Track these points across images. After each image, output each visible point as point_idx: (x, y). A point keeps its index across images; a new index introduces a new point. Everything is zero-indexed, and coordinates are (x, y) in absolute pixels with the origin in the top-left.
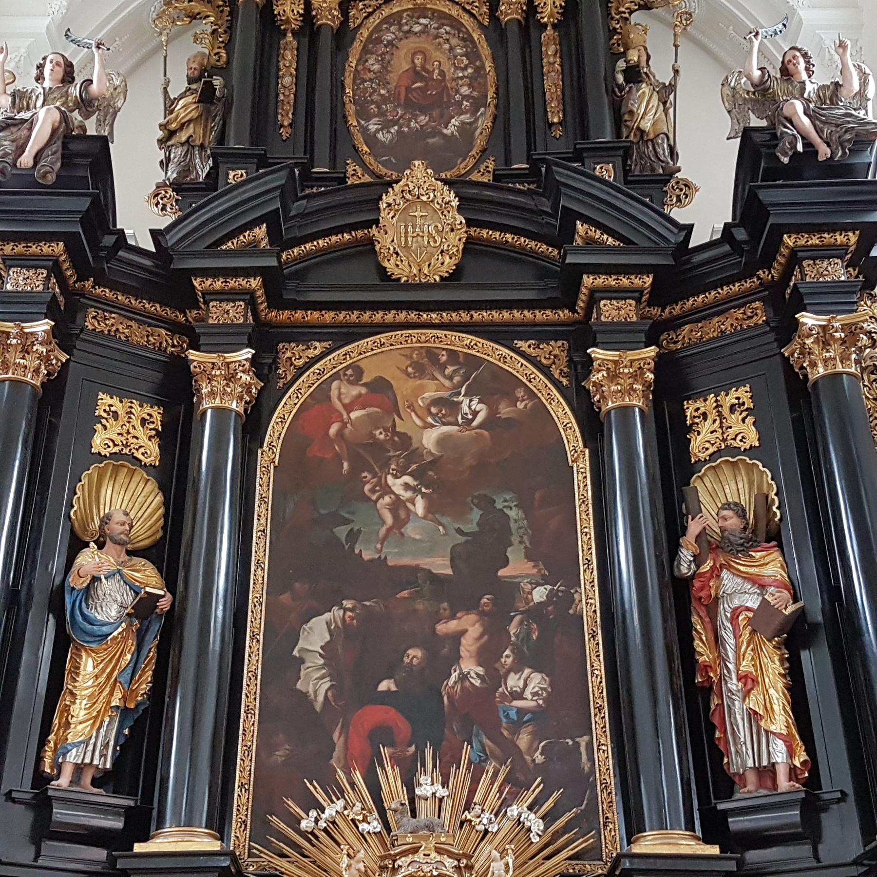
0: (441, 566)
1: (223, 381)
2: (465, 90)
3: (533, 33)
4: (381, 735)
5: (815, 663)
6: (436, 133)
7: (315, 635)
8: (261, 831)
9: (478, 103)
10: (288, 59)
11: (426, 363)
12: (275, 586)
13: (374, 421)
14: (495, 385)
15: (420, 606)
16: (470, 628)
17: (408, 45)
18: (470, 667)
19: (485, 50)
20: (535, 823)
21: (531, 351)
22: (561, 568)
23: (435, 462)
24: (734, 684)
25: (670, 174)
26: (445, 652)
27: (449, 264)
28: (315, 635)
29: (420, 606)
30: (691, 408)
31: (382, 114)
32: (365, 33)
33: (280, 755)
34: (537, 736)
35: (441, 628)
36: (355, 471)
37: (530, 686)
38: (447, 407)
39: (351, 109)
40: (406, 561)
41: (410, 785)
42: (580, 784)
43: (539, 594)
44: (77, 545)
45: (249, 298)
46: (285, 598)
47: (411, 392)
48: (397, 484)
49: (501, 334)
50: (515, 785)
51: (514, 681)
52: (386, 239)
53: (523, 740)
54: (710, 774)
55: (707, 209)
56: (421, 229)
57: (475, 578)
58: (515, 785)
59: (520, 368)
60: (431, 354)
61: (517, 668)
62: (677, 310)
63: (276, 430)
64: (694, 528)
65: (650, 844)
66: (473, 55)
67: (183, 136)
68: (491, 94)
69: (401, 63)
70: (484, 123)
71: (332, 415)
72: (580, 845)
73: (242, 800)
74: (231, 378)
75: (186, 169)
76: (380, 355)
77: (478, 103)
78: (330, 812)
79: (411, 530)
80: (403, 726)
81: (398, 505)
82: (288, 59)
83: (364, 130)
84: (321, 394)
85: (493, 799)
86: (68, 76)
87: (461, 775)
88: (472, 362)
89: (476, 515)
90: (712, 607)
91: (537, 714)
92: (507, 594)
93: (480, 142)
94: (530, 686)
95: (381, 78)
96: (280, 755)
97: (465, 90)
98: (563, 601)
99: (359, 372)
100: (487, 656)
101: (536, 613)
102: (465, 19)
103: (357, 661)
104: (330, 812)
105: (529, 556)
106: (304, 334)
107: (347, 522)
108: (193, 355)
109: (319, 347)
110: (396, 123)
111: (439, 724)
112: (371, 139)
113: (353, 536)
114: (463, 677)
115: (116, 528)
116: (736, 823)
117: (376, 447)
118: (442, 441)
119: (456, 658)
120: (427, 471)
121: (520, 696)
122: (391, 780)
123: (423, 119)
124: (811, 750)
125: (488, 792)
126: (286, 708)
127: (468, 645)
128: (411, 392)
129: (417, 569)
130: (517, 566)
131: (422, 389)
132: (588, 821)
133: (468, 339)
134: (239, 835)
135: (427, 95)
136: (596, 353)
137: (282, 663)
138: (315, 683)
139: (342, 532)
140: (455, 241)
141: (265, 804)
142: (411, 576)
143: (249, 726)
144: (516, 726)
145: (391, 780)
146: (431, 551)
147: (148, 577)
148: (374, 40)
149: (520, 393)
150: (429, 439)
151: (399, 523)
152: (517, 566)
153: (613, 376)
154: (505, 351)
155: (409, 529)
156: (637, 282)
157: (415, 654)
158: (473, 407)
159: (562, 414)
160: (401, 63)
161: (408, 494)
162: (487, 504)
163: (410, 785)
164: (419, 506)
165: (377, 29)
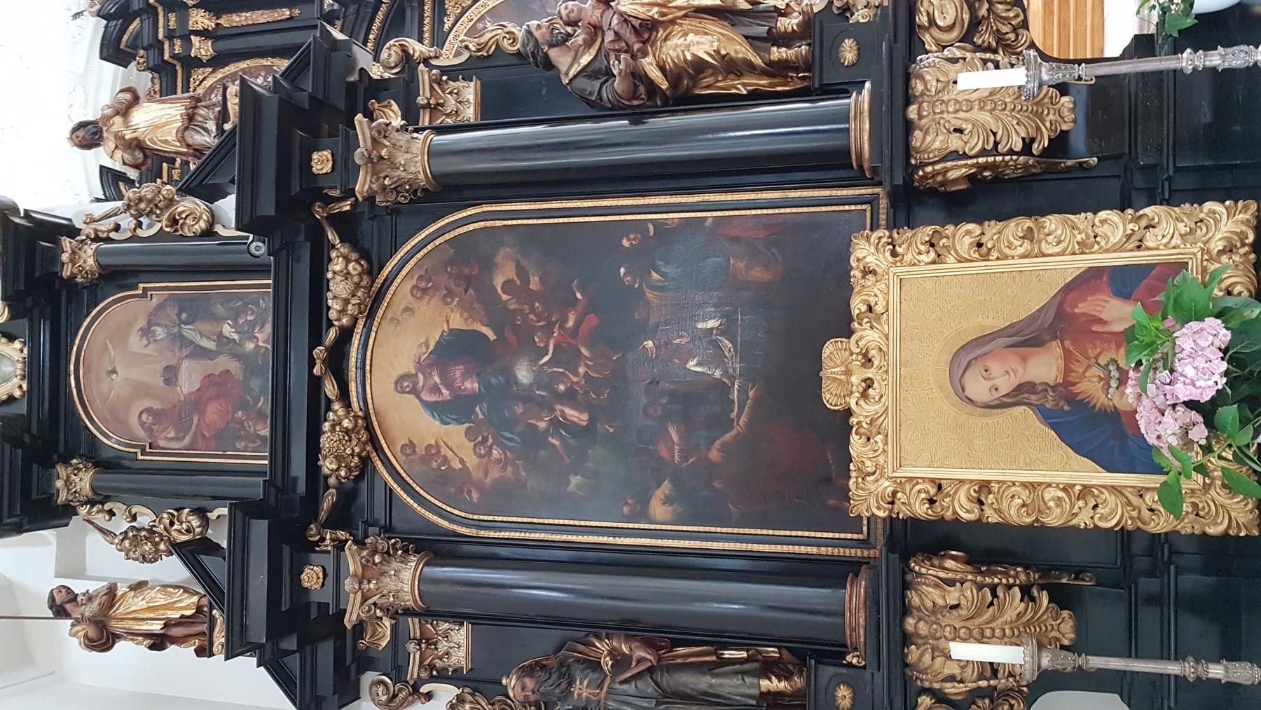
3: (220, 33)
21: (452, 19)
59: (465, 24)
68: (265, 62)
102: (207, 84)
149: (480, 26)
154: (451, 36)
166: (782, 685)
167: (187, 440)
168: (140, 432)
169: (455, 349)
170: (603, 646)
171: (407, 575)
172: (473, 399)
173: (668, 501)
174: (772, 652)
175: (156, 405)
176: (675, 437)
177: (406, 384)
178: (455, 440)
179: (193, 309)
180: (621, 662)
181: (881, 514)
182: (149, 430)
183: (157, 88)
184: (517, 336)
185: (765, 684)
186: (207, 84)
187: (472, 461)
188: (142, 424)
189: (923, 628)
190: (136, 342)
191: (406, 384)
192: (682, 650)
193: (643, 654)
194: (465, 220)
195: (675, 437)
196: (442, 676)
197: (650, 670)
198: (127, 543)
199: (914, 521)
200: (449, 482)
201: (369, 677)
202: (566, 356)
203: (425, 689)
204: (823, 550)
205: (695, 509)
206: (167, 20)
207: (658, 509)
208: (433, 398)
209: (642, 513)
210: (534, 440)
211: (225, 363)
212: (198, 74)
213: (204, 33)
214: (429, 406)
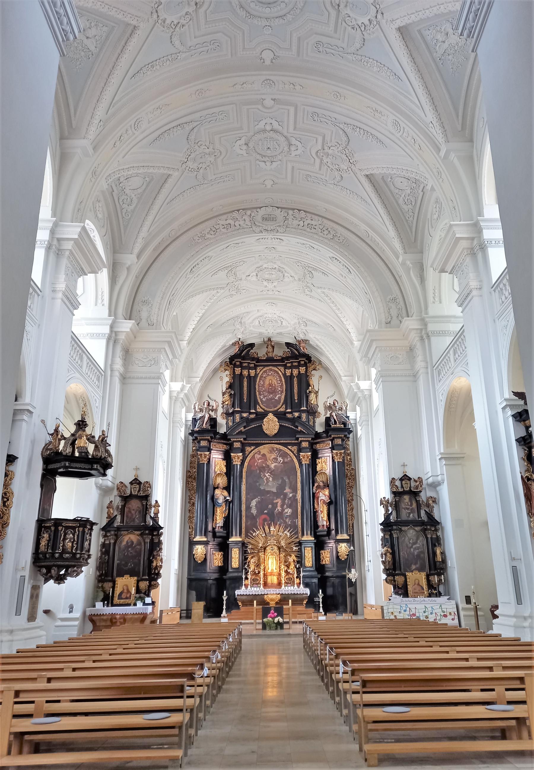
0: (274, 490)
1: (237, 458)
2: (279, 389)
4: (265, 520)
5: (332, 508)
6: (274, 399)
7: (254, 503)
8: (247, 536)
9: (282, 392)
10: (245, 384)
11: (272, 451)
12: (247, 494)
13: (263, 462)
14: (284, 455)
15: (271, 498)
16: (279, 501)
17: (268, 378)
18: (279, 508)
19: (283, 380)
20: (288, 534)
22: (295, 490)
23: (274, 470)
24: (319, 511)
25: (316, 412)
26: (275, 506)
27: (276, 431)
28: (254, 503)
29: (271, 498)
30: (318, 461)
31: (263, 394)
32: (260, 375)
33: (249, 523)
34: (289, 520)
35: (275, 501)
36: (260, 472)
37: (288, 511)
38: (276, 459)
39: (257, 393)
40: (269, 489)
41: (269, 528)
42: (296, 527)
43: (291, 495)
44: (215, 488)
45: (241, 441)
46: (249, 496)
47: (269, 456)
48: (267, 475)
49: (285, 445)
50: (286, 528)
51: (286, 511)
52: (264, 427)
53: (287, 520)
54: (315, 525)
55: (319, 428)
56: (271, 424)
57: (280, 493)
58: (286, 528)
60: (273, 449)
61: (286, 508)
62: (316, 441)
63: (246, 464)
64: (316, 485)
65: (305, 538)
66: (281, 380)
67: (227, 403)
69: (267, 382)
70: (283, 397)
71: (255, 461)
72: (295, 537)
73: (243, 530)
74: (238, 458)
75: (227, 410)
76: (264, 449)
77: (282, 392)
78: (257, 533)
79: (270, 484)
80: (268, 518)
81: (267, 479)
82: (245, 384)
83: (260, 398)
84: (253, 457)
85: (282, 530)
86: (209, 405)
87: (277, 527)
88: (280, 450)
89: (280, 481)
90: (318, 498)
91: (289, 516)
92: (285, 495)
93: (282, 401)
94: (288, 511)
95: (263, 386)
96: (249, 523)
97: (279, 389)
98: (294, 496)
99: (260, 452)
100: (282, 506)
101: (290, 498)
102: (279, 372)
103: (260, 507)
104: (257, 533)
105: (290, 488)
106: (250, 445)
107: (258, 482)
108: (232, 454)
109: (253, 447)
110: (266, 396)
111: (273, 518)
112: (261, 400)
113: (260, 485)
114: (278, 510)
115: (221, 486)
116: (318, 534)
117: (263, 467)
118: (275, 466)
119: (277, 507)
120: (272, 472)
121: (287, 513)
122: (266, 528)
123: (271, 396)
124: (330, 523)
125: (281, 529)
126: (250, 516)
127: (279, 504)
128: (269, 456)
129: (270, 491)
130: (287, 490)
131: (271, 456)
132: (297, 533)
133: (280, 446)
134: (243, 535)
135: (272, 390)
136: (301, 454)
137: (248, 508)
138: (254, 511)
139: (258, 484)
140: (277, 427)
141: (247, 532)
142: (269, 492)
143: (244, 519)
144: (286, 518)
145: (266, 528)
146: (273, 488)
147: (226, 493)
148: (261, 377)
150: (272, 466)
151: (267, 482)
152: (287, 490)
153: (304, 457)
155: (270, 484)
156: (308, 439)
157: (270, 506)
158: (280, 459)
159: (295, 460)
160: (267, 382)
161: (268, 477)
162: (282, 478)
163: (269, 528)
164: (271, 479)
165: (262, 374)
169: (132, 542)
177: (130, 538)
178: (124, 543)
179: (140, 512)
183: (278, 358)
184: (133, 548)
186: (279, 372)
190: (137, 506)
191: (130, 538)
194: (143, 544)
200: (121, 543)
202: (131, 553)
206: (296, 362)
210: (124, 550)
211: (134, 516)
212: (282, 369)
213: (292, 373)
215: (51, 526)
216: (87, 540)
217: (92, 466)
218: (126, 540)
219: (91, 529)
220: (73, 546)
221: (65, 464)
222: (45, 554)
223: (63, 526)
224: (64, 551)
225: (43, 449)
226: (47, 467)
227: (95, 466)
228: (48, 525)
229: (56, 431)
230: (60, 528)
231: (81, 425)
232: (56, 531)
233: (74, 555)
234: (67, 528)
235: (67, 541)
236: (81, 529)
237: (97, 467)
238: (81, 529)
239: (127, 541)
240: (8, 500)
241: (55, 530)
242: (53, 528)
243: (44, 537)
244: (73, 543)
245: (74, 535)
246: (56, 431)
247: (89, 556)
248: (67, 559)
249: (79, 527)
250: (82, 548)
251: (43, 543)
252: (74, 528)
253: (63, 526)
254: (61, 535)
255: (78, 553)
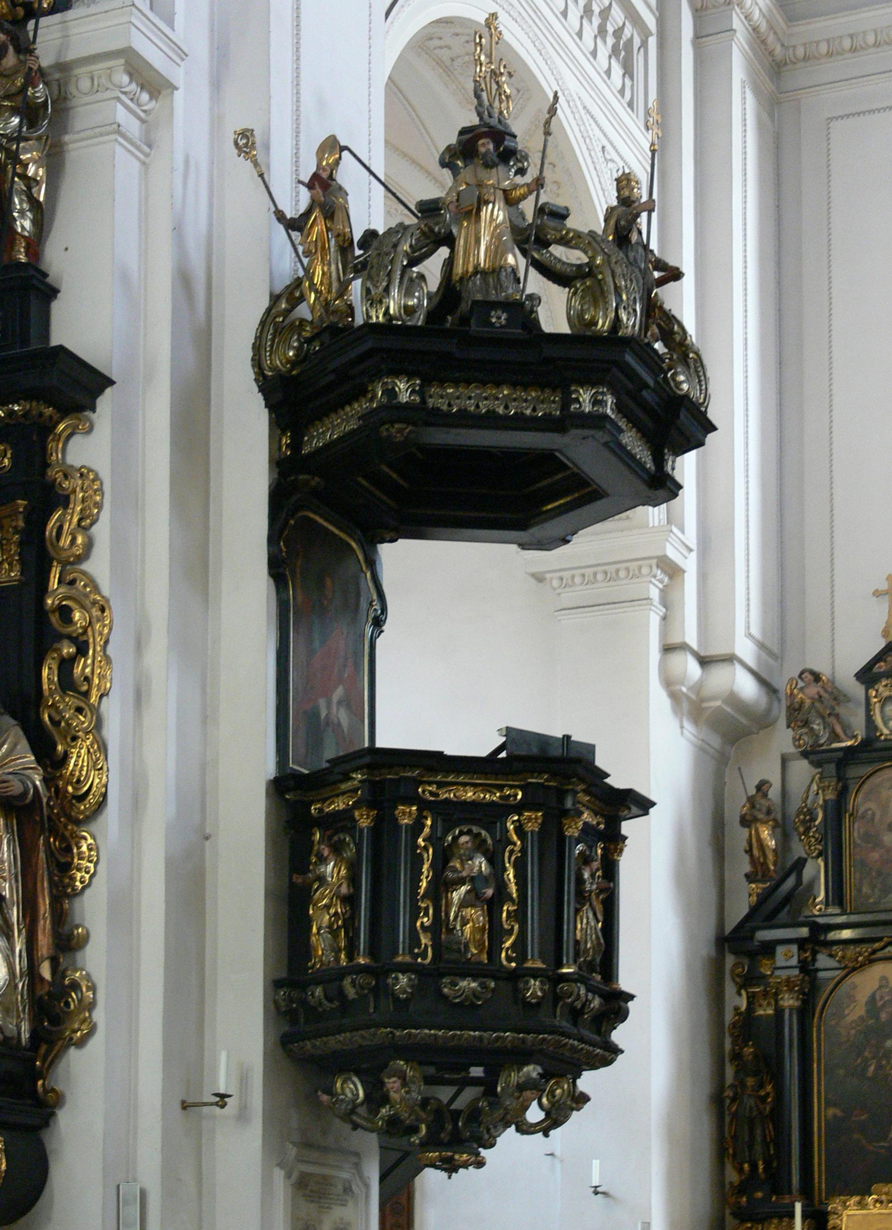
166: (761, 1170)
167: (859, 842)
168: (862, 810)
170: (769, 1088)
171: (791, 1002)
172: (878, 1018)
173: (835, 1116)
174: (775, 1164)
175: (877, 817)
176: (863, 1118)
180: (763, 1099)
181: (829, 1209)
182: (863, 817)
185: (760, 1163)
187: (849, 1019)
188: (866, 811)
189: (784, 1224)
192: (771, 1127)
193: (768, 1109)
195: (863, 1118)
196: (752, 1000)
197: (760, 1113)
198: (802, 817)
199: (827, 1221)
201: (746, 961)
203: (743, 992)
204: (817, 1185)
205: (834, 1129)
207: (831, 1111)
208: (878, 997)
209: (828, 1104)
214: (874, 994)
215: (347, 813)
216: (582, 897)
217: (566, 402)
218: (863, 996)
219: (614, 840)
220: (495, 932)
221: (391, 393)
222: (332, 978)
223: (424, 806)
224: (450, 960)
225: (263, 323)
226: (296, 445)
227: (585, 398)
228: (339, 805)
229: (323, 184)
230: (406, 814)
231: (484, 146)
232: (385, 825)
233: (516, 977)
234: (451, 814)
235: (457, 895)
236: (533, 820)
237: (596, 402)
238: (533, 820)
239: (872, 1000)
240: (82, 650)
241: (376, 831)
242: (364, 821)
243: (321, 879)
244: (493, 907)
245: (495, 860)
246: (323, 184)
247: (616, 1005)
248: (466, 1011)
249: (519, 808)
250: (555, 944)
251: (323, 916)
252: (490, 815)
253: (424, 806)
254: (417, 862)
255: (535, 974)
